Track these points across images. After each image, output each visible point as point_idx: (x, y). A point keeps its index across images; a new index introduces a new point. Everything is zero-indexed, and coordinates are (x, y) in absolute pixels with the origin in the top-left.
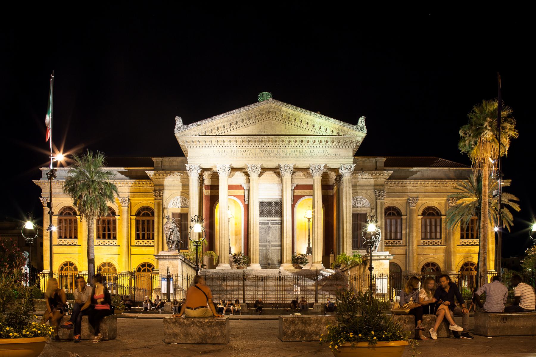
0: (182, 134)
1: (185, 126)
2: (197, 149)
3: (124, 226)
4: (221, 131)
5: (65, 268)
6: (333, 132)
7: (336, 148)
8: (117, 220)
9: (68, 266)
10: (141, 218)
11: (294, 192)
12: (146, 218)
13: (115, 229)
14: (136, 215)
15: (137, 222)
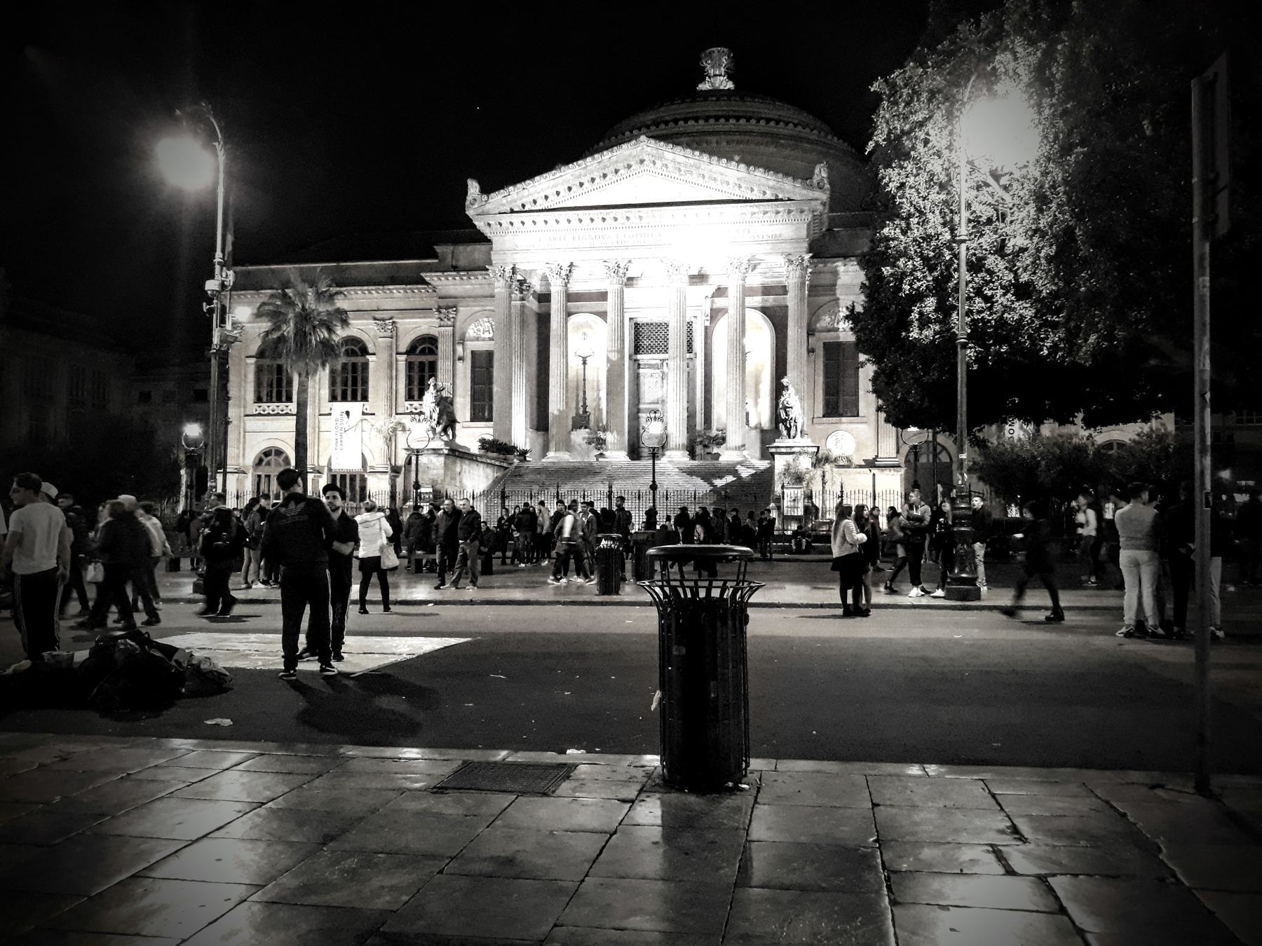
0: (480, 210)
1: (485, 197)
2: (508, 237)
3: (383, 376)
4: (554, 202)
5: (266, 460)
6: (765, 193)
7: (773, 223)
8: (371, 365)
9: (272, 458)
10: (417, 359)
11: (713, 302)
12: (424, 358)
13: (365, 382)
14: (408, 353)
15: (410, 366)
